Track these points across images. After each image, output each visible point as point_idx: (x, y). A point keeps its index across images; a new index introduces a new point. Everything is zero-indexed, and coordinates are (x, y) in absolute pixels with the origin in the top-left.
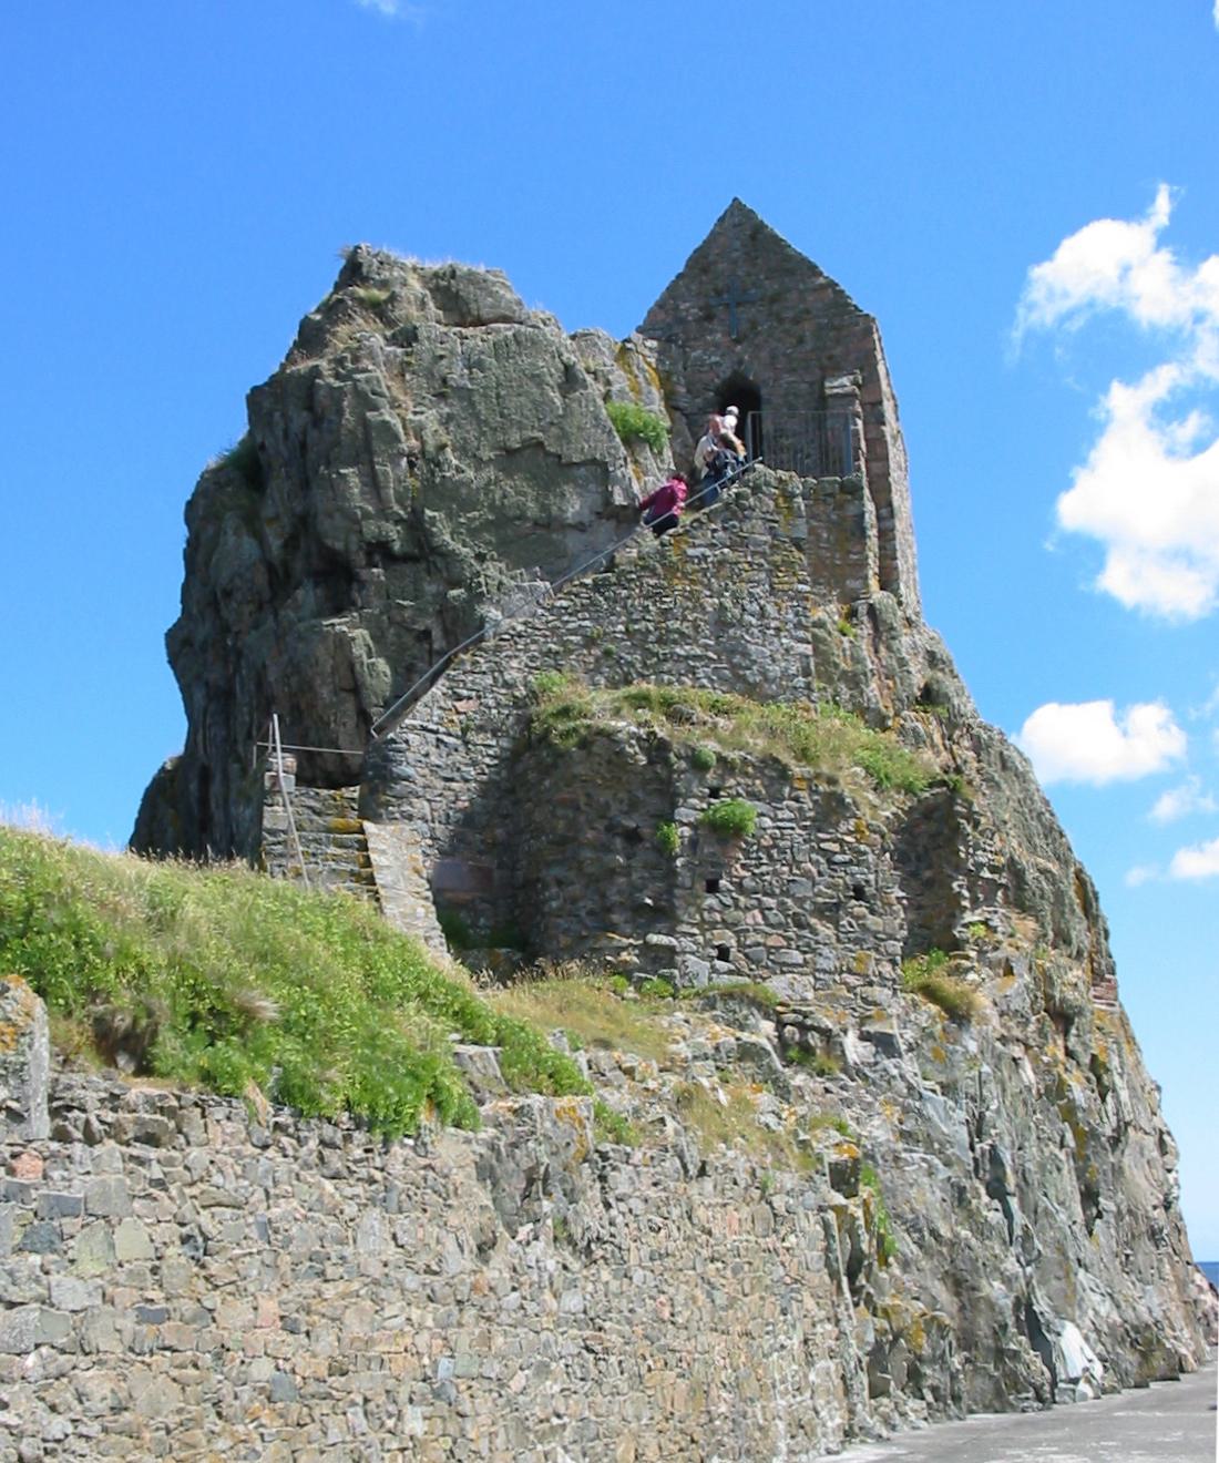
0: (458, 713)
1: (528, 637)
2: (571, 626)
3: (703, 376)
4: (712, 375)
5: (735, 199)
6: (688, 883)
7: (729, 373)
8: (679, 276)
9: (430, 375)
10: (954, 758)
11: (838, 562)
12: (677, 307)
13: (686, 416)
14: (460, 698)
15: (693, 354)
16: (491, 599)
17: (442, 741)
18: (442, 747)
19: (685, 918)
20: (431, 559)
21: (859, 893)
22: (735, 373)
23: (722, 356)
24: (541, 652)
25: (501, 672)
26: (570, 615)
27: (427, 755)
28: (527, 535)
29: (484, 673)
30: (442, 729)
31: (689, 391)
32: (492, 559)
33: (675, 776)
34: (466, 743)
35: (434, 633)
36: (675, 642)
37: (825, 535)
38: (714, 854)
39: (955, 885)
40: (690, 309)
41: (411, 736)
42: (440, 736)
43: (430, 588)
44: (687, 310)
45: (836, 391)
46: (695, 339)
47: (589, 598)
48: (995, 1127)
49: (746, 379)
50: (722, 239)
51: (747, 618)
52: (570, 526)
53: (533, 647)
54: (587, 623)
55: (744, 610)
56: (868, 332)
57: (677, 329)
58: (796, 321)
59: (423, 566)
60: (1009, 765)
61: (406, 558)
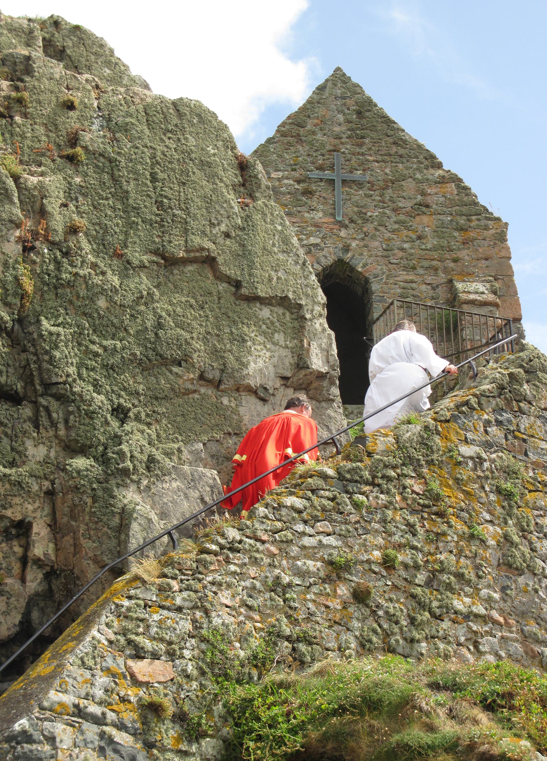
0: (136, 682)
1: (246, 551)
2: (307, 541)
7: (330, 261)
8: (269, 141)
9: (52, 125)
14: (139, 654)
16: (138, 482)
17: (111, 741)
18: (109, 752)
20: (43, 401)
23: (324, 238)
24: (264, 583)
25: (207, 612)
26: (305, 522)
28: (188, 392)
29: (179, 609)
30: (111, 716)
32: (137, 418)
34: (149, 746)
35: (35, 529)
36: (449, 587)
41: (60, 729)
42: (107, 729)
43: (36, 452)
44: (279, 180)
45: (472, 297)
47: (333, 499)
49: (352, 269)
50: (321, 111)
53: (253, 571)
54: (326, 540)
55: (533, 550)
56: (502, 237)
59: (27, 411)
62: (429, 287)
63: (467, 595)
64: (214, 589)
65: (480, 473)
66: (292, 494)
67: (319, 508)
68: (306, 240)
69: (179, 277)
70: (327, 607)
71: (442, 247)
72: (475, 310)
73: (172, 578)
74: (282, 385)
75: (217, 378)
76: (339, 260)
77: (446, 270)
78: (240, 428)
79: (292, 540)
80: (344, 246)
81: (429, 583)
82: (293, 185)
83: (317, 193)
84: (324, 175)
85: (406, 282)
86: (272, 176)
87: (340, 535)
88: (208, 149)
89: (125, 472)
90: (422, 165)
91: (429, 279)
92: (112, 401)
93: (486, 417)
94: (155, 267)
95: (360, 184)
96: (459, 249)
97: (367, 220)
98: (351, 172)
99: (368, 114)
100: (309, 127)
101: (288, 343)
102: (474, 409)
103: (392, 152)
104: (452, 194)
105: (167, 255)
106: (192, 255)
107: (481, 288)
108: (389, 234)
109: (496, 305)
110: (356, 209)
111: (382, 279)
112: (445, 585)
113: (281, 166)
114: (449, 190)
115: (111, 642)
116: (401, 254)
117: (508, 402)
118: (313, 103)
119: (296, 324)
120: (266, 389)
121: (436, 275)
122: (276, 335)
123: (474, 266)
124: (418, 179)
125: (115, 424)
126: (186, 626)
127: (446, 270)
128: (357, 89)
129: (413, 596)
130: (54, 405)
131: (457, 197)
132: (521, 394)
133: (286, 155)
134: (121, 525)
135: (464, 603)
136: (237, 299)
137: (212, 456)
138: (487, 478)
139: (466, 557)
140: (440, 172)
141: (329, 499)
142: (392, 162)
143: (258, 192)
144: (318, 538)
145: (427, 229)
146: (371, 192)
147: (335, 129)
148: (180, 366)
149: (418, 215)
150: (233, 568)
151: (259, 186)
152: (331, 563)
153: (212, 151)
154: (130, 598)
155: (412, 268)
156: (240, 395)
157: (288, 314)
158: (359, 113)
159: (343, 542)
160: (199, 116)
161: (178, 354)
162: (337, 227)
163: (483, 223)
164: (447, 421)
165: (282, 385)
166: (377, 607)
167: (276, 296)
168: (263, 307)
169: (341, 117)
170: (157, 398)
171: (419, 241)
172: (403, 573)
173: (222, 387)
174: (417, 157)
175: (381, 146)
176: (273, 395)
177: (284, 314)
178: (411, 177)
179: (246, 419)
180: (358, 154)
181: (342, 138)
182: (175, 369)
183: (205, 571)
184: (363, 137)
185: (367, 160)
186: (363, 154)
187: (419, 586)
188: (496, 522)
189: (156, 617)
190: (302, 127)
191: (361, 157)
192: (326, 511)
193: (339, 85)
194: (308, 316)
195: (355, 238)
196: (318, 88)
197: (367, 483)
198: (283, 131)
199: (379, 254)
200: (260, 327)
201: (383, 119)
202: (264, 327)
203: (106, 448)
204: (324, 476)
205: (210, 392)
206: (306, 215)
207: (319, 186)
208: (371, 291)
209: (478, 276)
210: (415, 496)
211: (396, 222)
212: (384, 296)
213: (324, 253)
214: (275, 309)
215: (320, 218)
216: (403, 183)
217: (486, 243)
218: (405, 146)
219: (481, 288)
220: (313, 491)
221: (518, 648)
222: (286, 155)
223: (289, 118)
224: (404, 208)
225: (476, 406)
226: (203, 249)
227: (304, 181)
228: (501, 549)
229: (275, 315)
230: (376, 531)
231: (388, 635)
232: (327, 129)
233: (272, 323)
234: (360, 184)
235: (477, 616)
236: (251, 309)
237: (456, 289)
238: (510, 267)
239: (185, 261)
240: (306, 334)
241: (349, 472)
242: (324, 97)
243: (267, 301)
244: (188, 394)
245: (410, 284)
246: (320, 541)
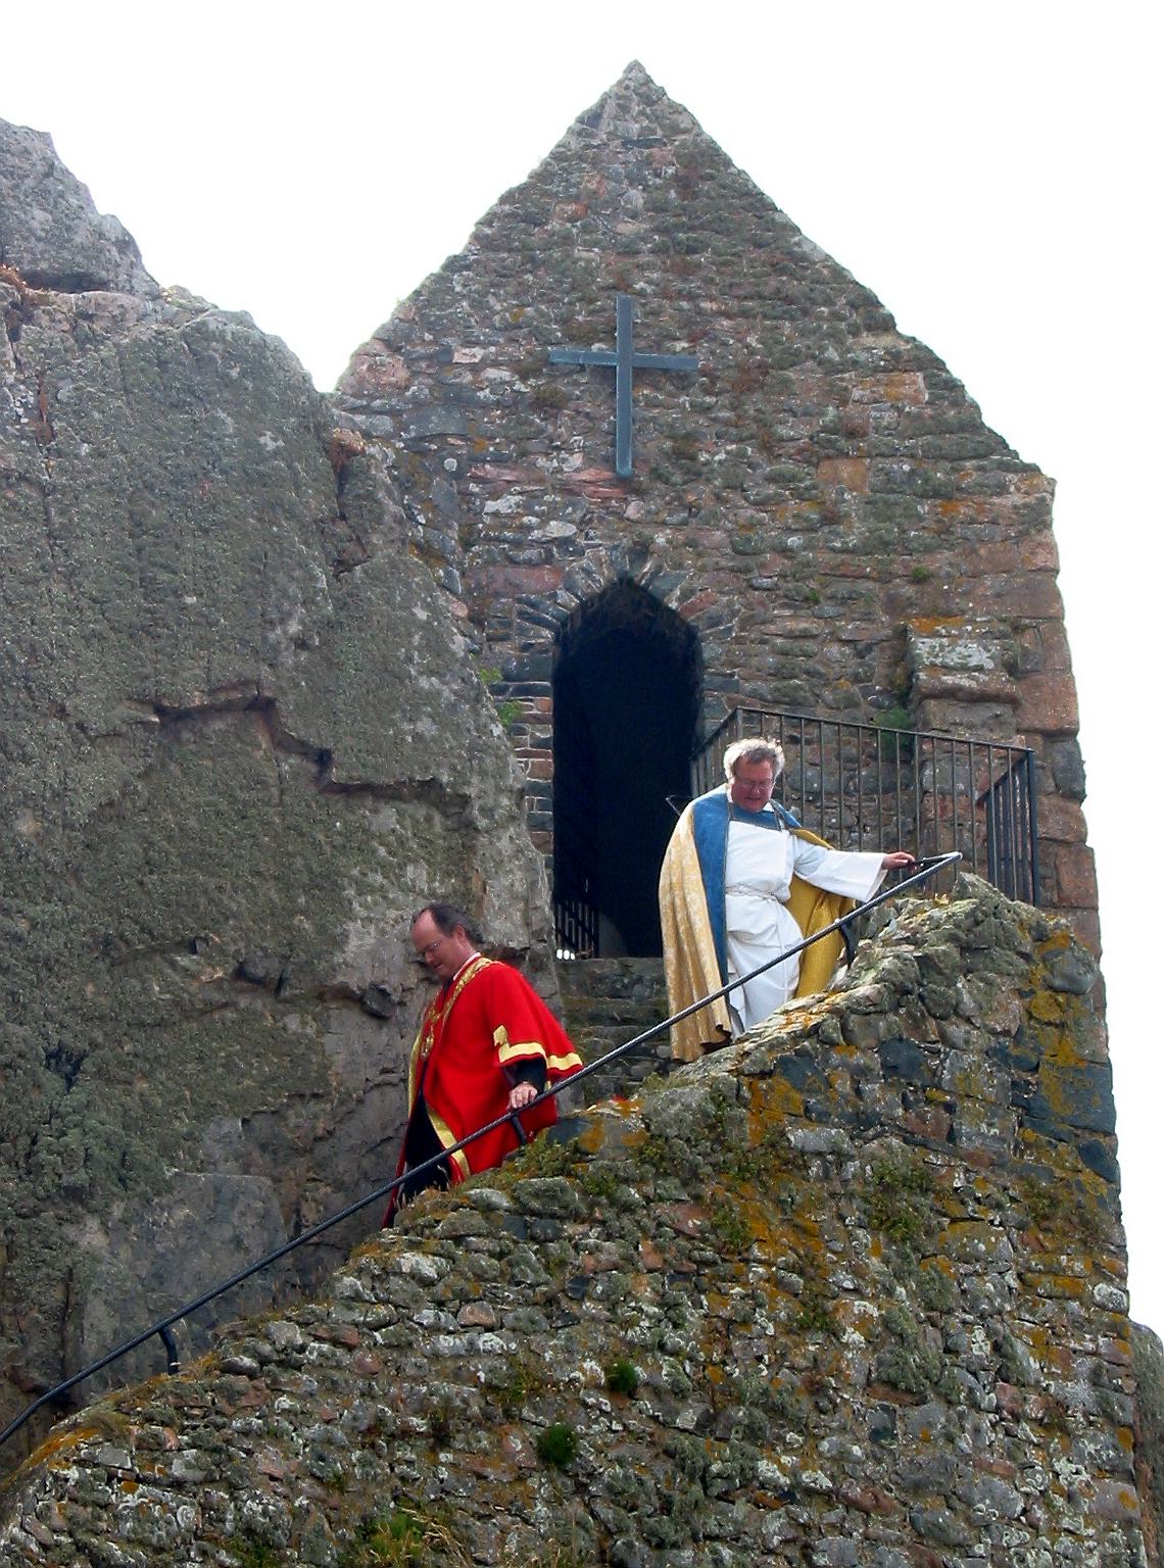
2: (445, 1342)
3: (520, 575)
5: (635, 66)
7: (602, 579)
8: (454, 265)
12: (448, 351)
15: (491, 506)
16: (103, 1214)
22: (625, 583)
23: (583, 523)
25: (233, 1488)
26: (440, 1304)
28: (211, 1008)
31: (476, 619)
32: (101, 1073)
44: (475, 369)
49: (656, 604)
52: (346, 995)
56: (1037, 517)
58: (818, 452)
62: (847, 650)
63: (789, 1449)
64: (248, 1444)
65: (838, 1187)
66: (413, 1246)
67: (470, 1274)
68: (539, 527)
69: (192, 747)
70: (481, 1477)
71: (886, 544)
72: (956, 713)
73: (163, 1424)
74: (422, 980)
75: (275, 976)
76: (621, 580)
77: (894, 605)
78: (323, 1079)
79: (410, 1344)
80: (636, 543)
81: (705, 1425)
82: (511, 384)
83: (572, 405)
84: (588, 356)
85: (791, 636)
86: (457, 358)
87: (514, 1330)
88: (262, 440)
89: (75, 1194)
90: (843, 325)
91: (848, 628)
92: (46, 1037)
93: (858, 1059)
94: (140, 733)
95: (681, 378)
96: (928, 550)
97: (699, 474)
98: (658, 346)
99: (705, 186)
100: (554, 225)
101: (437, 884)
102: (833, 1044)
103: (766, 291)
104: (915, 401)
105: (166, 703)
106: (222, 697)
107: (978, 655)
108: (750, 512)
109: (1013, 702)
110: (668, 444)
111: (730, 630)
112: (741, 1429)
113: (480, 332)
114: (906, 390)
115: (45, 1547)
116: (781, 564)
117: (917, 1025)
118: (567, 159)
119: (456, 840)
120: (383, 992)
121: (868, 617)
122: (410, 869)
123: (964, 594)
124: (829, 361)
125: (52, 1081)
126: (187, 1514)
127: (894, 605)
128: (680, 118)
129: (670, 1454)
131: (929, 411)
132: (947, 1003)
133: (492, 300)
134: (67, 1304)
135: (782, 1468)
136: (321, 792)
137: (263, 1147)
138: (851, 1196)
139: (792, 1368)
140: (887, 340)
141: (492, 1255)
142: (765, 317)
143: (375, 531)
144: (465, 1338)
145: (847, 496)
146: (709, 400)
147: (622, 228)
148: (194, 952)
149: (828, 457)
150: (285, 1402)
151: (379, 520)
152: (490, 1387)
153: (271, 446)
154: (81, 1463)
155: (806, 599)
156: (328, 1009)
157: (437, 818)
158: (684, 184)
159: (520, 1344)
160: (241, 358)
162: (616, 492)
163: (991, 478)
164: (764, 1075)
165: (422, 980)
166: (590, 1475)
167: (411, 780)
168: (381, 805)
169: (637, 197)
170: (142, 1025)
171: (826, 529)
172: (647, 1404)
173: (286, 993)
174: (828, 302)
175: (738, 273)
176: (402, 1004)
177: (429, 819)
178: (814, 357)
179: (339, 1060)
180: (680, 294)
181: (638, 252)
182: (183, 960)
183: (229, 1410)
184: (691, 251)
185: (700, 312)
186: (691, 297)
187: (685, 1431)
188: (869, 1291)
189: (131, 1500)
190: (536, 225)
191: (685, 304)
192: (486, 1280)
193: (636, 109)
194: (482, 823)
195: (664, 524)
196: (580, 120)
197: (577, 1218)
198: (487, 236)
199: (723, 563)
200: (374, 851)
201: (745, 202)
202: (382, 851)
203: (34, 1142)
204: (488, 1209)
205: (259, 1005)
206: (541, 462)
207: (576, 384)
208: (703, 661)
209: (971, 622)
210: (682, 1242)
211: (771, 479)
212: (732, 675)
213: (584, 562)
214: (409, 808)
215: (577, 470)
216: (791, 374)
217: (999, 532)
218: (800, 272)
219: (978, 655)
220: (459, 1240)
222: (492, 300)
223: (503, 200)
224: (792, 439)
225: (837, 1036)
226: (245, 683)
227: (535, 372)
228: (875, 1350)
229: (408, 822)
230: (593, 1319)
231: (609, 1533)
232: (602, 229)
233: (401, 842)
234: (681, 380)
235: (810, 1492)
236: (354, 813)
237: (914, 659)
238: (1056, 596)
239: (204, 713)
240: (476, 864)
241: (537, 1195)
242: (595, 143)
243: (389, 792)
244: (211, 1012)
245: (801, 642)
246: (471, 1343)
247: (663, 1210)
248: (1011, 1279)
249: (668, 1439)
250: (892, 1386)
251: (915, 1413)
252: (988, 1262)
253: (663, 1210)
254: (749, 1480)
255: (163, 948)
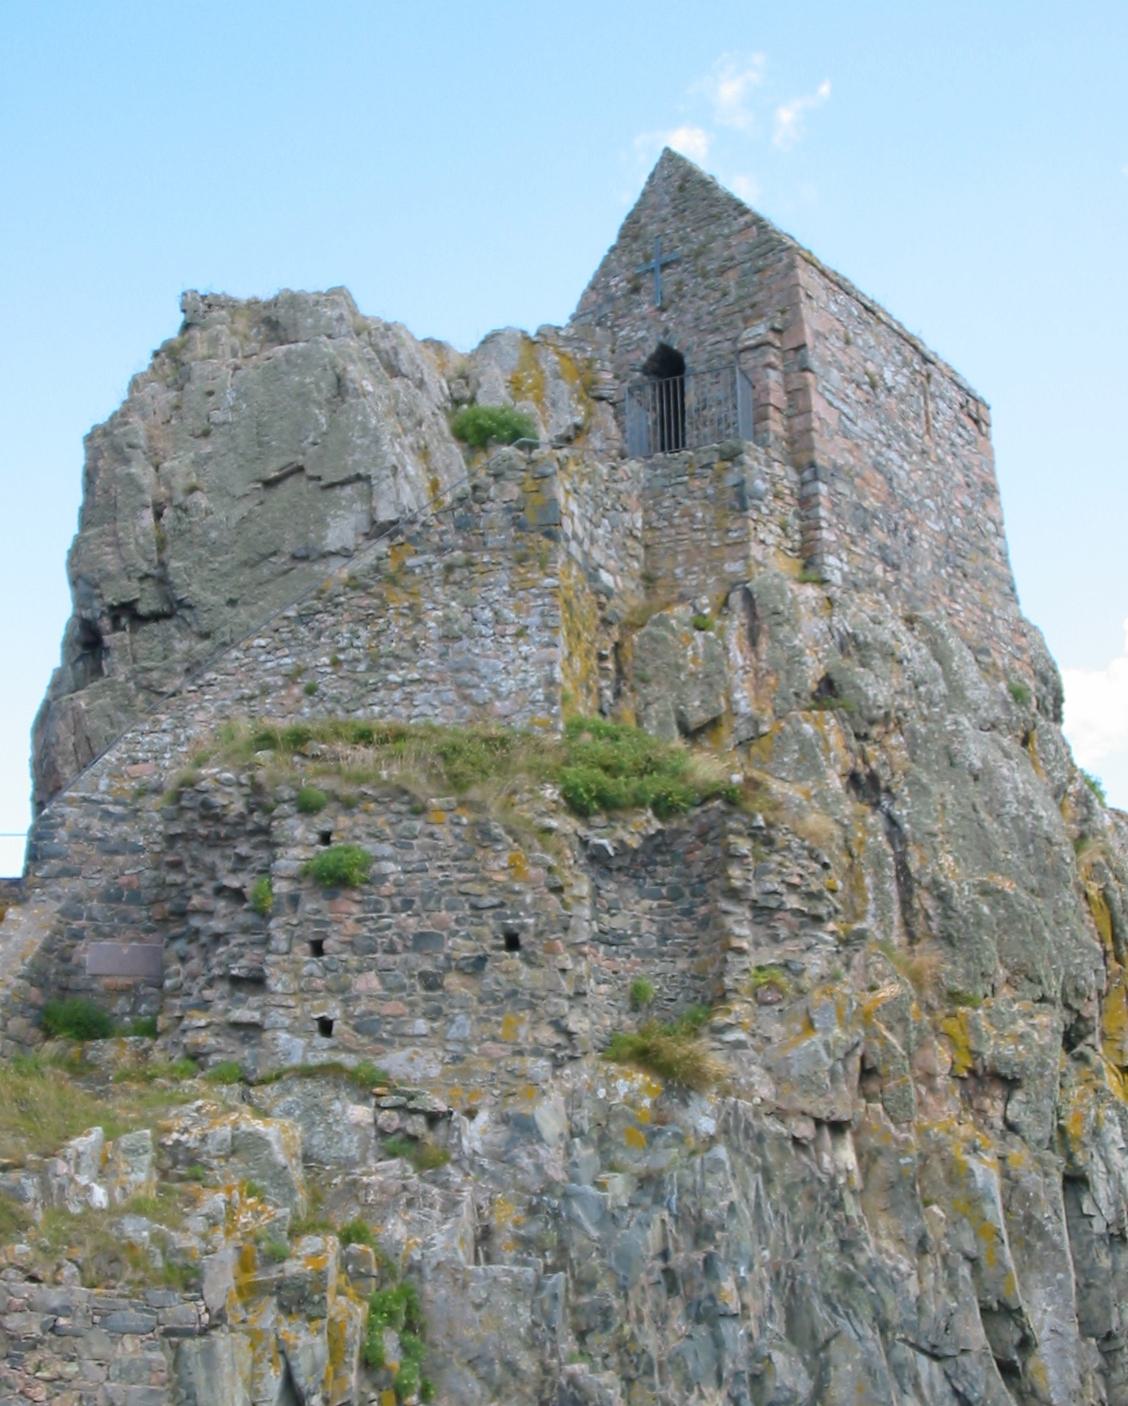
2: (269, 665)
4: (639, 353)
6: (283, 946)
7: (653, 349)
8: (613, 250)
10: (866, 762)
11: (715, 544)
13: (613, 404)
14: (135, 762)
15: (623, 333)
19: (279, 988)
21: (512, 943)
23: (648, 329)
27: (88, 828)
29: (164, 731)
33: (275, 823)
36: (388, 667)
37: (700, 515)
38: (318, 912)
39: (729, 921)
40: (618, 284)
46: (623, 316)
48: (722, 1228)
51: (478, 627)
53: (224, 694)
54: (288, 660)
57: (607, 309)
60: (958, 760)
61: (156, 617)
81: (370, 669)
116: (709, 318)
130: (186, 613)
161: (272, 548)
182: (273, 559)
221: (452, 696)
247: (355, 602)
248: (506, 588)
249: (355, 676)
250: (449, 638)
251: (457, 645)
252: (496, 584)
253: (355, 602)
254: (386, 682)
255: (265, 557)
